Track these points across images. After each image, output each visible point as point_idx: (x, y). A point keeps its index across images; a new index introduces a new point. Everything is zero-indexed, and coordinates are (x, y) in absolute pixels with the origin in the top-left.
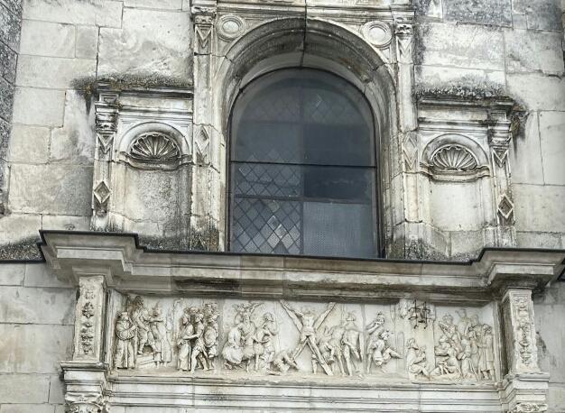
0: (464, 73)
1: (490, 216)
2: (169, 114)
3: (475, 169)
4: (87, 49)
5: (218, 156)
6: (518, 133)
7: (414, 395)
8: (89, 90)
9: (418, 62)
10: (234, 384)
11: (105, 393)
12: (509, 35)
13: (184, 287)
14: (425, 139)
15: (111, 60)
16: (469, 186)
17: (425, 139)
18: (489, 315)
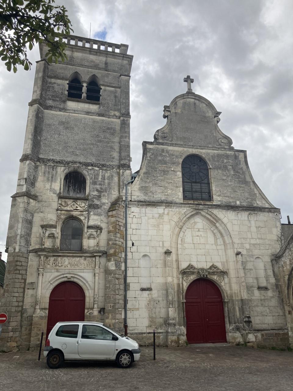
0: (95, 223)
1: (96, 245)
2: (53, 230)
3: (94, 237)
4: (42, 220)
5: (60, 237)
6: (101, 232)
7: (83, 271)
8: (43, 227)
9: (88, 222)
10: (60, 269)
11: (43, 271)
12: (101, 217)
13: (54, 256)
14: (88, 234)
15: (46, 222)
16: (94, 240)
17: (88, 234)
18: (94, 259)
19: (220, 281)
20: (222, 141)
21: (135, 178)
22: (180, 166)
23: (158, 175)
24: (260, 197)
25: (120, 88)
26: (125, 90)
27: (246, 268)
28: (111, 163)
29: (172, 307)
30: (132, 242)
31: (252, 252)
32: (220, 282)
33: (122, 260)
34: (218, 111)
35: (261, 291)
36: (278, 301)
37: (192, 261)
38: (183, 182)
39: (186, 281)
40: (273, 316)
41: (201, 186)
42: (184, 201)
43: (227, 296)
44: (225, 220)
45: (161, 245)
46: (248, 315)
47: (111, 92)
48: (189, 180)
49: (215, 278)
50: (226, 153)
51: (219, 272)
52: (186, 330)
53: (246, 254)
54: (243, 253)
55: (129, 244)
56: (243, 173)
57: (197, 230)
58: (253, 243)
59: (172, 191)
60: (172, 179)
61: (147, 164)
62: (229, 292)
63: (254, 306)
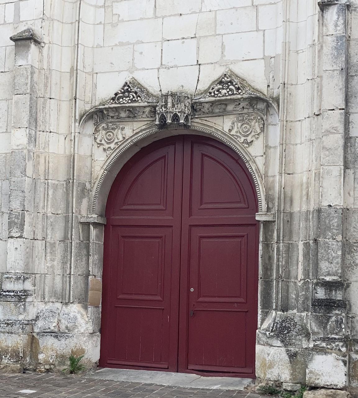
19: (242, 139)
29: (21, 237)
32: (245, 142)
37: (137, 69)
43: (269, 199)
46: (329, 274)
51: (245, 99)
62: (277, 182)
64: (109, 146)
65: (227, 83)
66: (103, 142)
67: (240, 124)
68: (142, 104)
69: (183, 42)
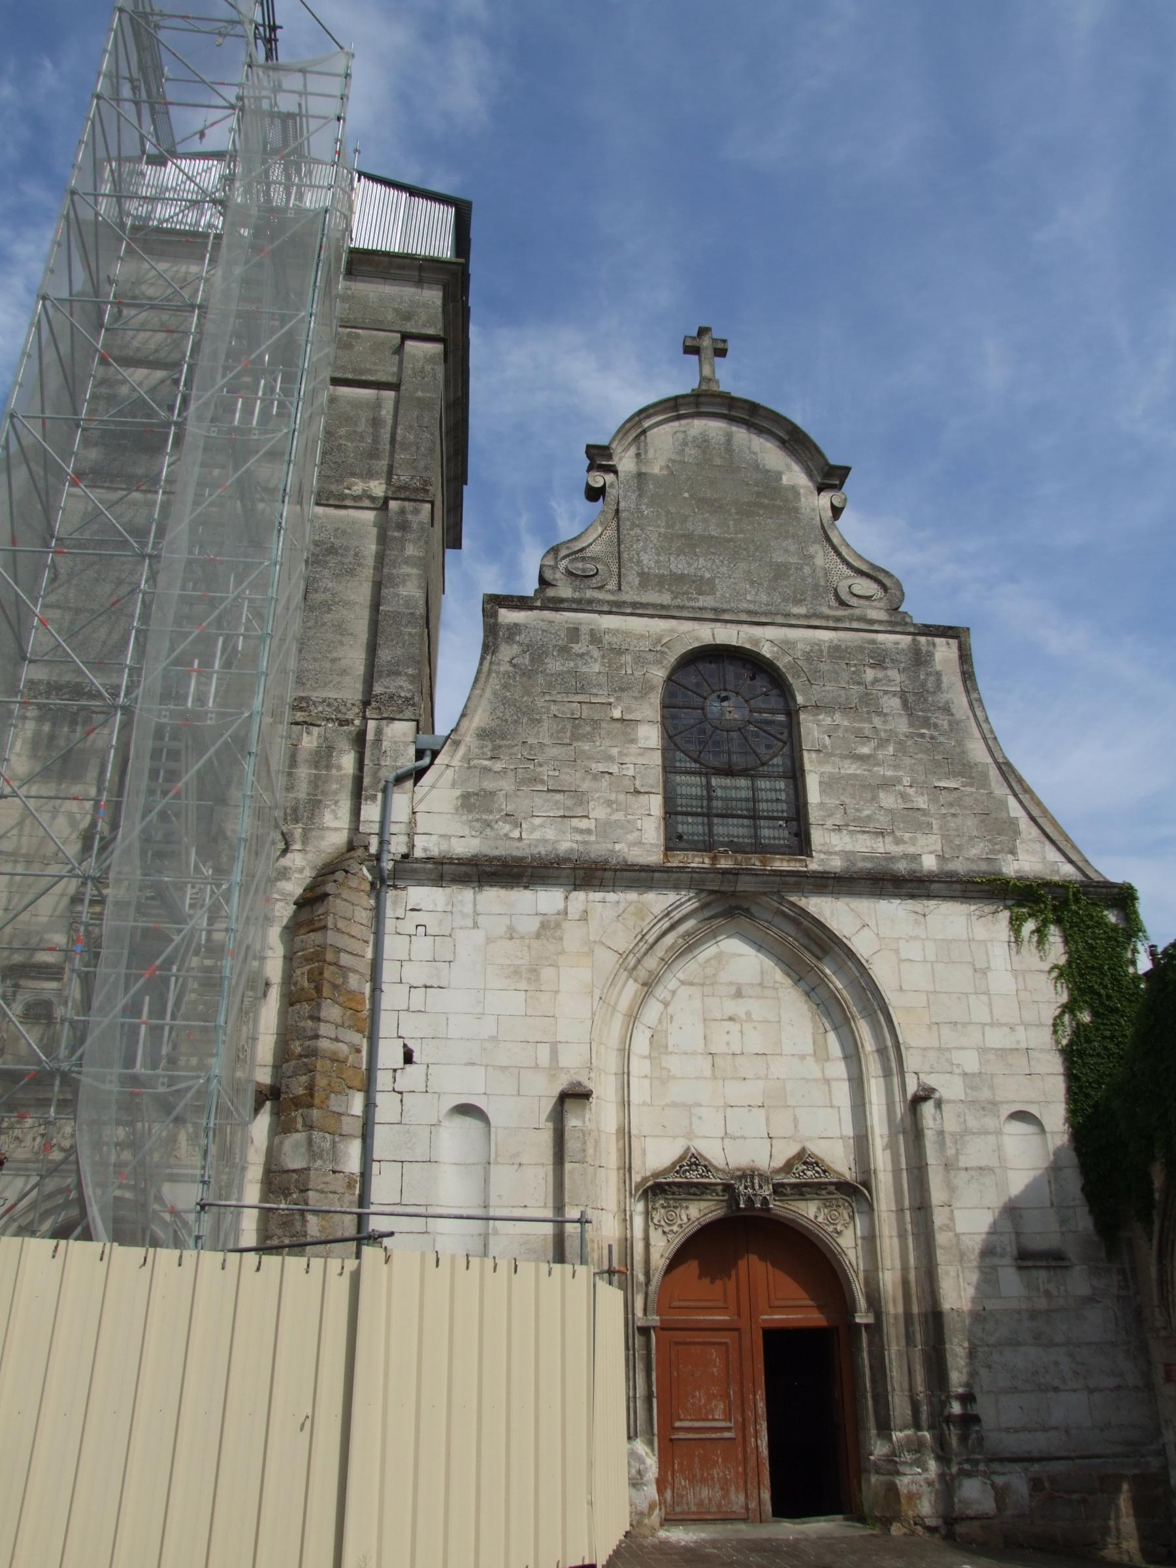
20: (857, 589)
21: (435, 754)
22: (656, 698)
23: (546, 741)
24: (1035, 831)
25: (396, 387)
26: (420, 394)
27: (962, 1164)
28: (332, 695)
30: (405, 1046)
31: (991, 1087)
33: (355, 1127)
34: (833, 461)
35: (1034, 1272)
36: (1116, 1318)
37: (697, 1137)
38: (669, 769)
39: (667, 1229)
40: (1091, 1391)
41: (754, 789)
42: (666, 856)
44: (861, 945)
45: (544, 1058)
47: (356, 404)
48: (696, 761)
49: (809, 1211)
50: (873, 642)
52: (655, 1459)
53: (963, 1098)
54: (943, 1092)
55: (389, 1054)
56: (951, 730)
57: (733, 990)
58: (999, 1046)
59: (609, 810)
60: (610, 758)
61: (495, 693)
63: (995, 1346)
64: (671, 1228)
65: (812, 1164)
66: (663, 1223)
67: (826, 1211)
68: (713, 1181)
69: (750, 1111)
